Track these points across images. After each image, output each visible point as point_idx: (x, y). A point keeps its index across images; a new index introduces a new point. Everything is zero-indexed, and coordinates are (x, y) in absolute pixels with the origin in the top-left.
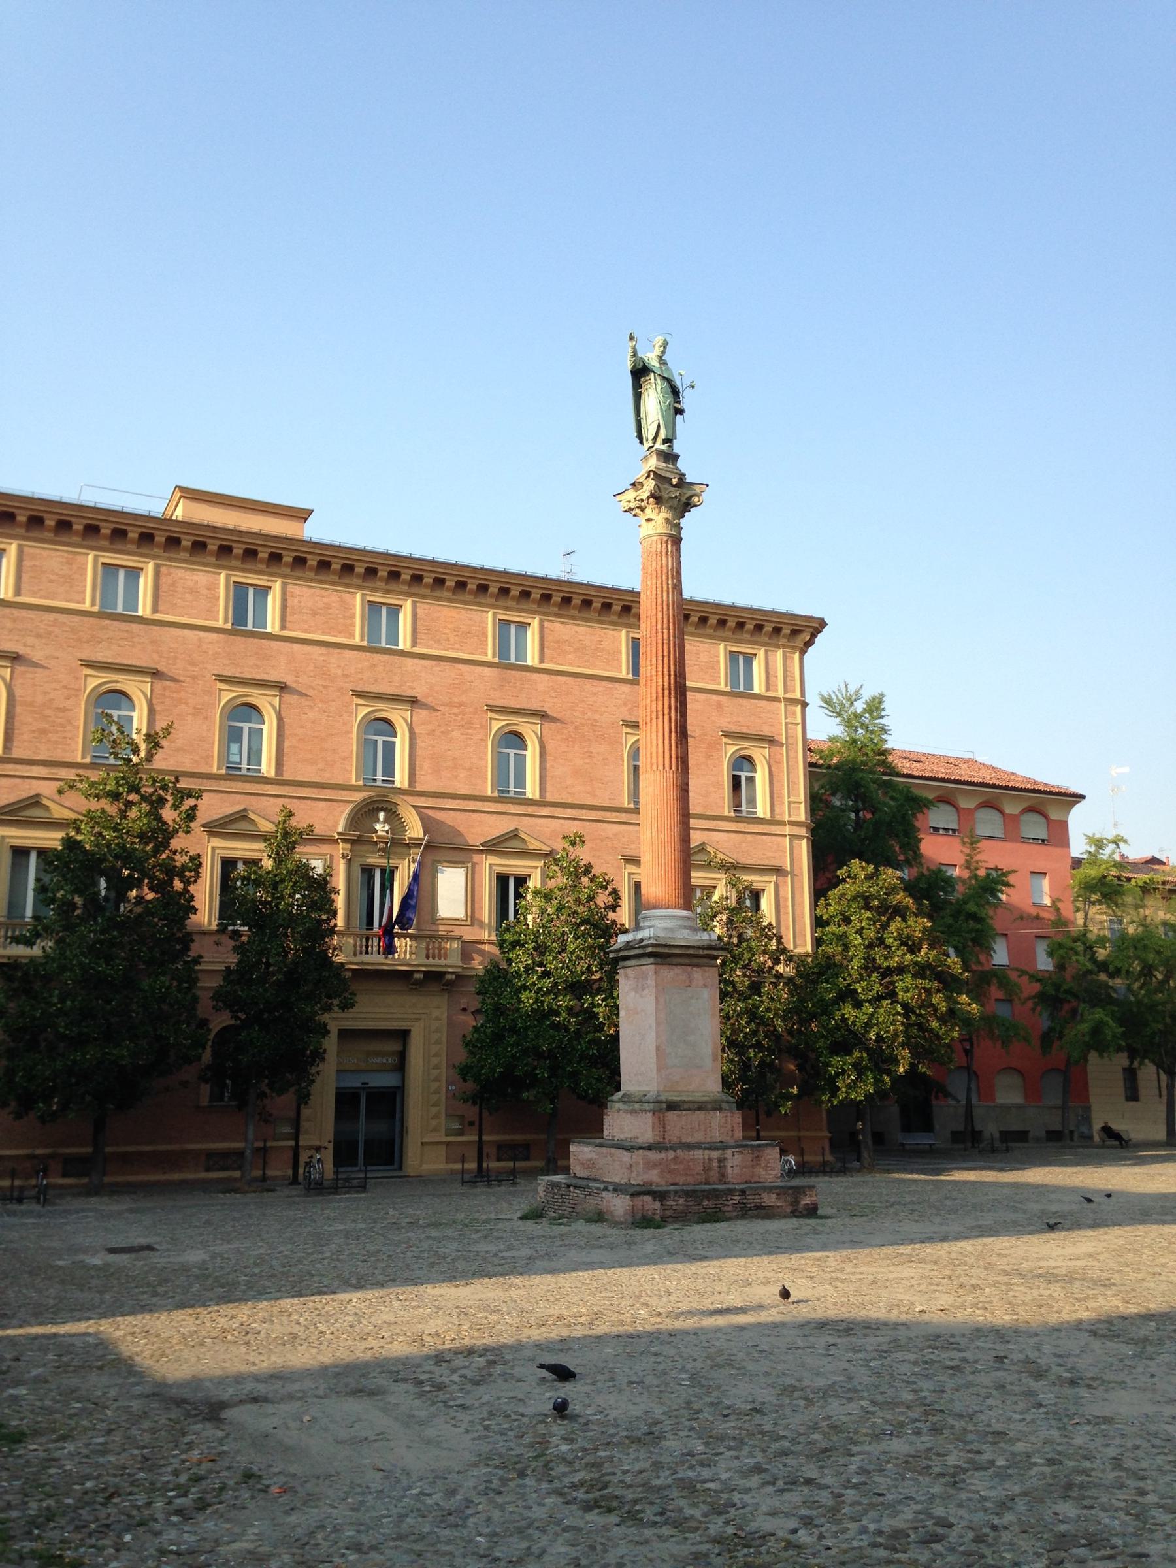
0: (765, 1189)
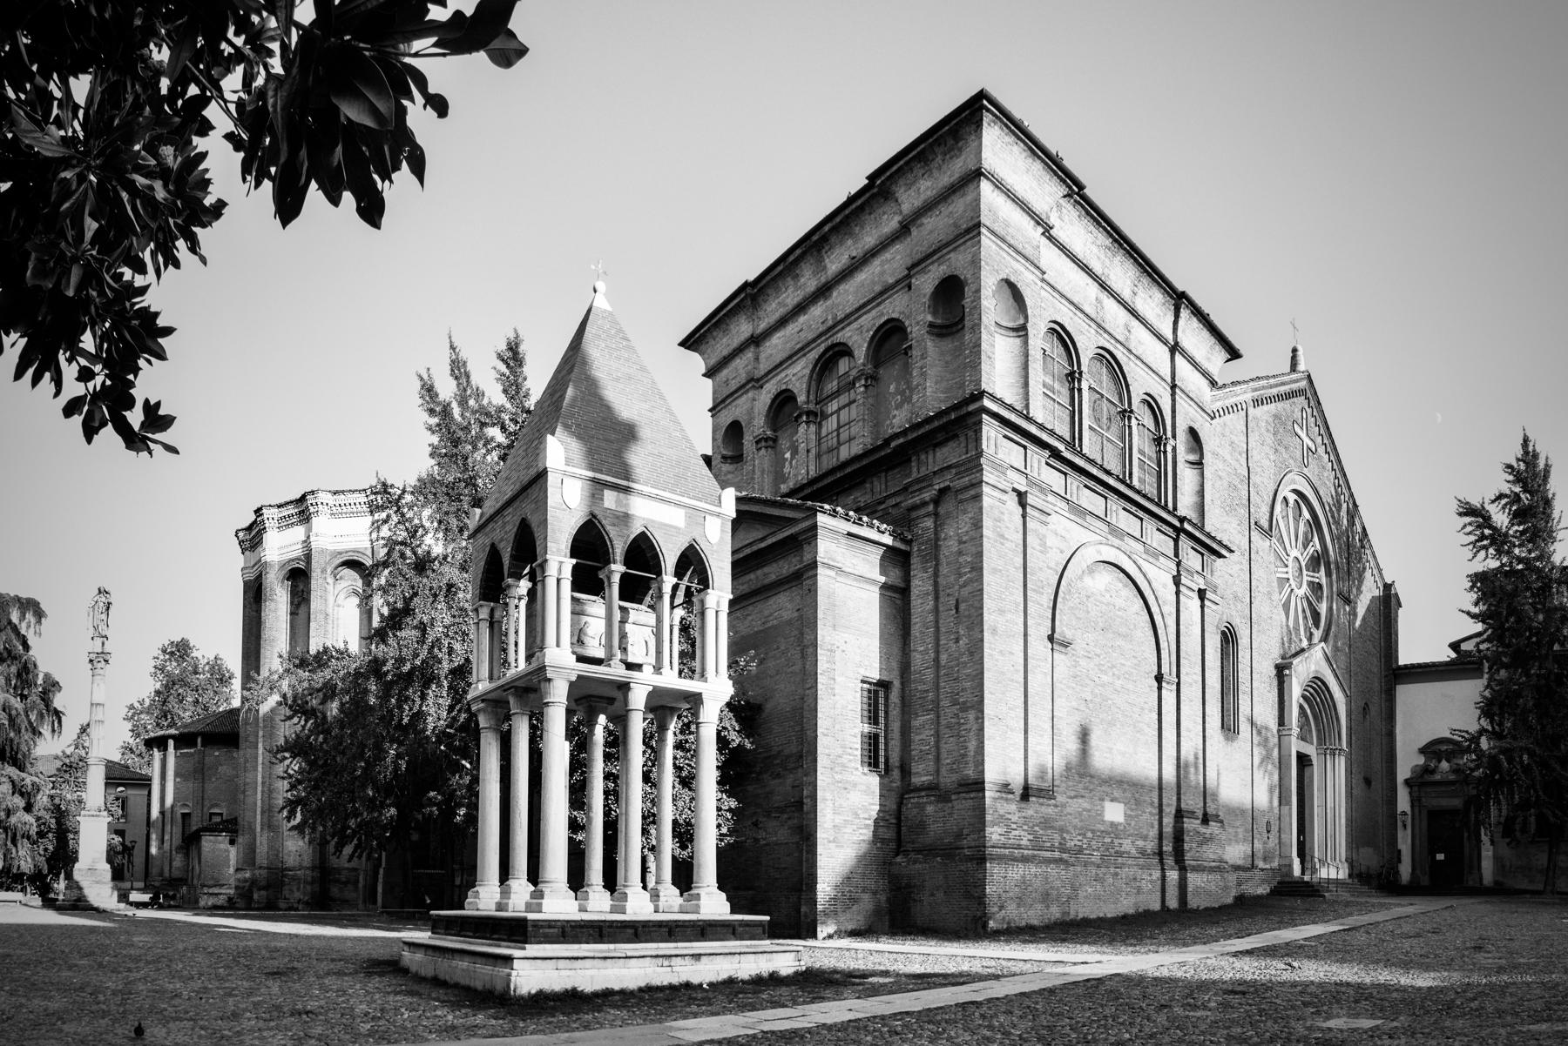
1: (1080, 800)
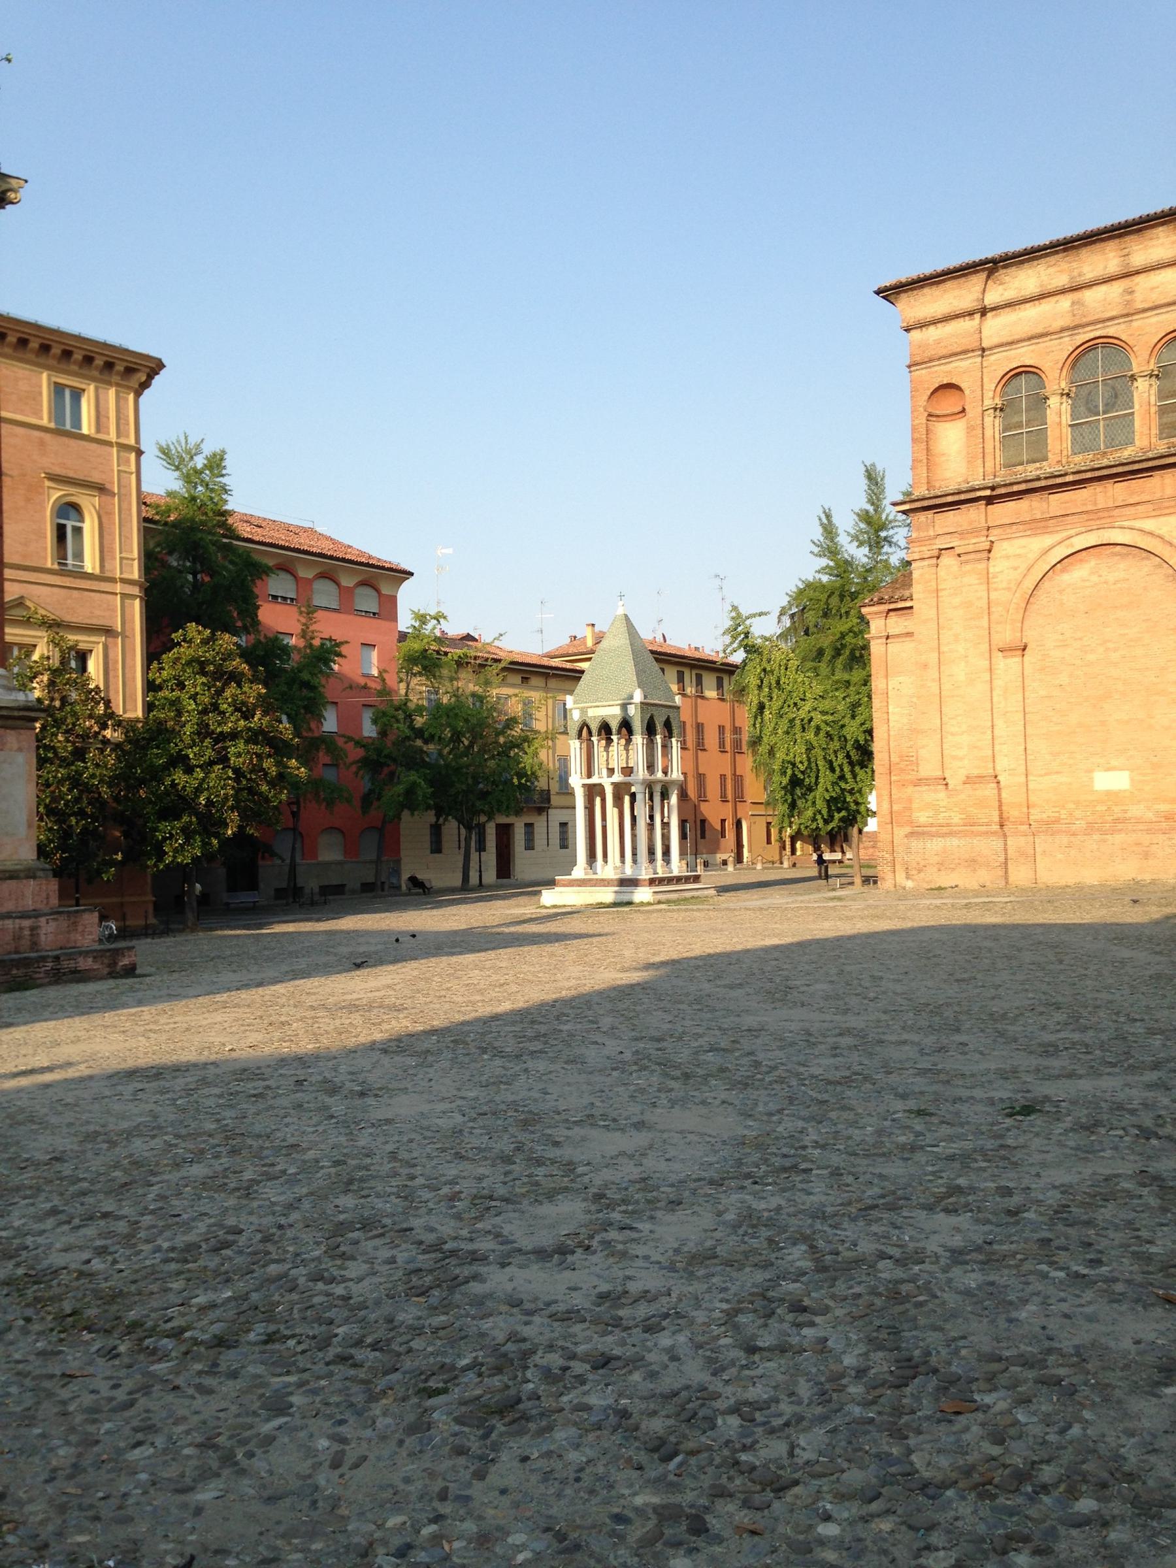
0: (80, 953)
1: (1054, 777)
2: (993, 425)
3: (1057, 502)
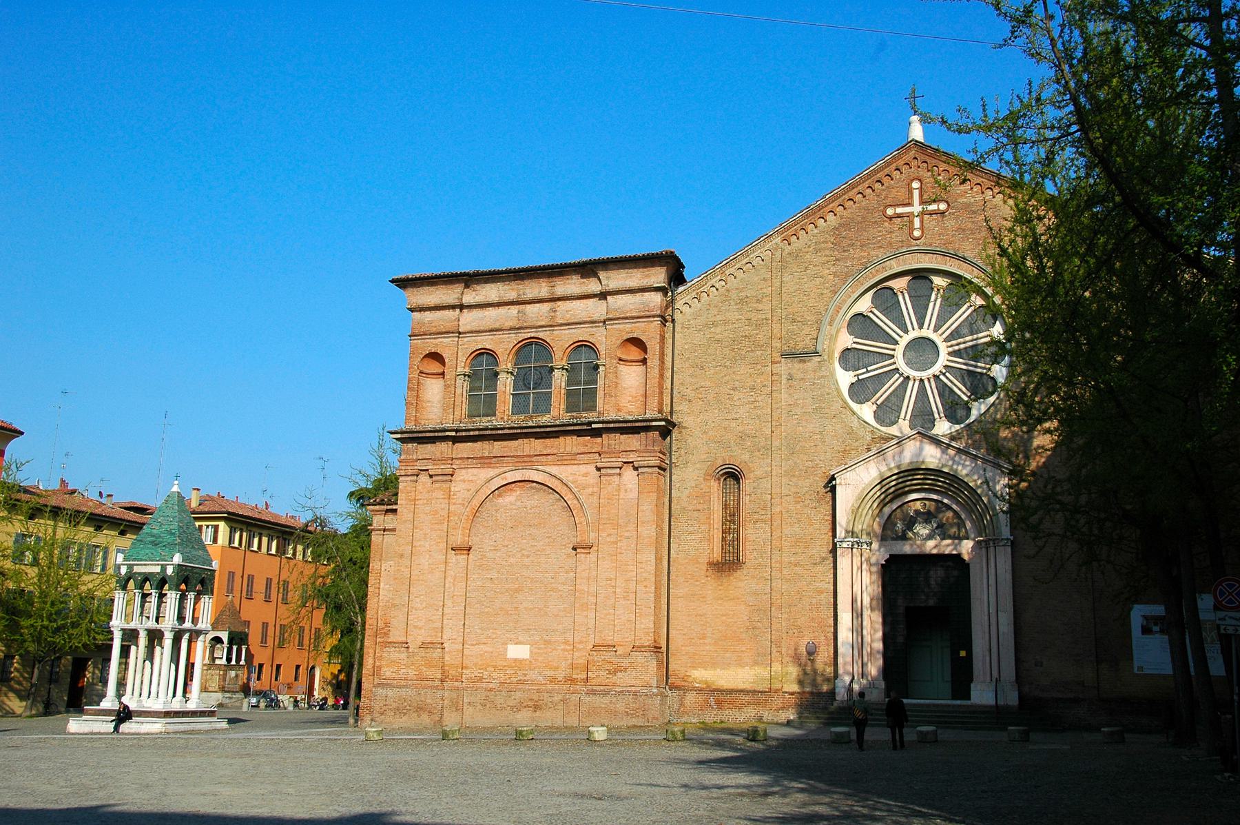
2: (463, 386)
3: (498, 447)
